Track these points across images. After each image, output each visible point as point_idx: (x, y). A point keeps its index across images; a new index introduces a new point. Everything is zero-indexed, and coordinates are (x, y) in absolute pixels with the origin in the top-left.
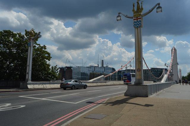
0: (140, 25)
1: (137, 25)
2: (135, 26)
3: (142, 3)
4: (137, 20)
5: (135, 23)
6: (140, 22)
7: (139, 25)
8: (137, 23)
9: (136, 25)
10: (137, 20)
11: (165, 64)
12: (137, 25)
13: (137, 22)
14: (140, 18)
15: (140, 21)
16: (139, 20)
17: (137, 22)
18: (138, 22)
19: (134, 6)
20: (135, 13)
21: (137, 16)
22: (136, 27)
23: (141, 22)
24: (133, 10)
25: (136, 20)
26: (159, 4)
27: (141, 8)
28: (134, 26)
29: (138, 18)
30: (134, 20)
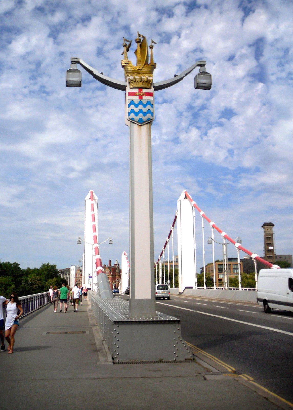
1: (141, 115)
2: (132, 115)
4: (141, 98)
5: (132, 107)
6: (149, 107)
7: (145, 114)
9: (137, 114)
10: (141, 98)
12: (141, 115)
13: (140, 103)
14: (151, 94)
15: (149, 102)
16: (145, 99)
17: (140, 103)
18: (145, 106)
20: (127, 72)
21: (140, 85)
22: (137, 118)
25: (137, 98)
28: (129, 114)
30: (131, 94)
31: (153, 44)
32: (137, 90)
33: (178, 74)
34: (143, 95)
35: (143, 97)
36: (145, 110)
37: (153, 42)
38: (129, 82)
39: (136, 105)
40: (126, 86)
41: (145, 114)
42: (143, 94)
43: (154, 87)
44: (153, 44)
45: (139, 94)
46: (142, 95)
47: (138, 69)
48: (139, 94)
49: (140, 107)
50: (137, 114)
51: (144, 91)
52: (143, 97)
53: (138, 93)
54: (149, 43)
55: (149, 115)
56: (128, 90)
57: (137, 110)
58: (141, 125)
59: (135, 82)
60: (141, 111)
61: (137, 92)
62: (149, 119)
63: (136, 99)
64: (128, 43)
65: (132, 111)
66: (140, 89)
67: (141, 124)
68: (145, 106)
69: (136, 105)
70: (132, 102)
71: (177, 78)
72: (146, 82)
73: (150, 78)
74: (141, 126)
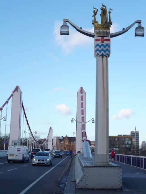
0: (107, 52)
1: (102, 52)
2: (98, 52)
3: (110, 13)
4: (103, 42)
5: (98, 47)
6: (107, 47)
7: (105, 52)
8: (102, 47)
9: (100, 52)
10: (103, 42)
11: (72, 120)
12: (102, 52)
13: (102, 45)
16: (105, 43)
18: (105, 47)
19: (95, 13)
20: (96, 28)
21: (102, 35)
22: (100, 54)
23: (109, 47)
24: (95, 22)
26: (139, 22)
27: (108, 22)
29: (105, 38)
31: (111, 11)
32: (100, 38)
33: (125, 28)
35: (104, 42)
36: (105, 49)
37: (110, 9)
39: (100, 47)
41: (105, 52)
44: (111, 11)
49: (102, 47)
50: (100, 52)
51: (105, 38)
52: (104, 42)
54: (108, 10)
57: (100, 49)
59: (99, 33)
60: (102, 50)
62: (107, 54)
63: (100, 43)
64: (96, 10)
65: (98, 50)
66: (102, 37)
68: (105, 47)
69: (100, 47)
70: (98, 45)
71: (124, 31)
73: (108, 31)
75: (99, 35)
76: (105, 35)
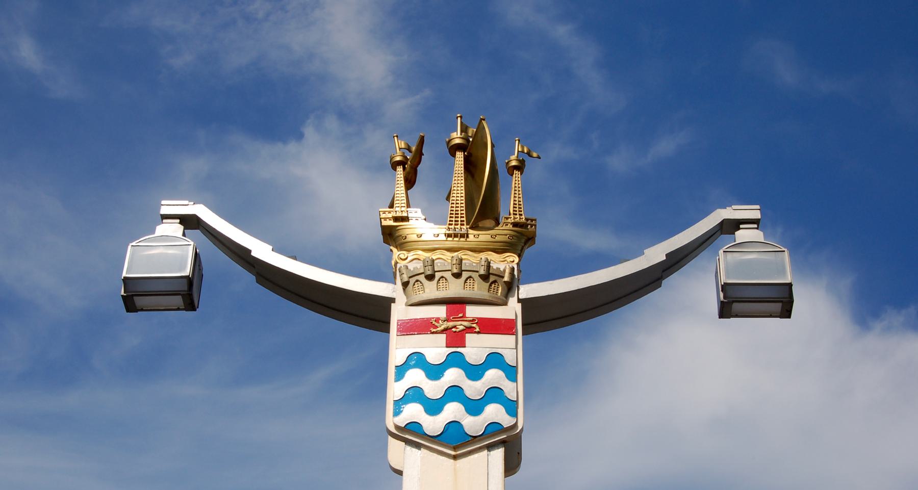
4: (456, 339)
7: (474, 407)
10: (456, 339)
17: (455, 360)
21: (455, 289)
22: (433, 424)
32: (440, 311)
34: (470, 330)
35: (469, 337)
36: (474, 389)
38: (406, 279)
40: (393, 300)
42: (466, 324)
43: (519, 301)
45: (451, 324)
46: (461, 328)
47: (449, 236)
48: (451, 324)
49: (453, 375)
51: (472, 311)
52: (469, 337)
53: (447, 320)
55: (494, 412)
56: (399, 313)
58: (453, 453)
60: (454, 393)
61: (437, 320)
67: (455, 448)
69: (434, 372)
72: (481, 276)
74: (455, 458)
75: (431, 290)
76: (479, 289)
